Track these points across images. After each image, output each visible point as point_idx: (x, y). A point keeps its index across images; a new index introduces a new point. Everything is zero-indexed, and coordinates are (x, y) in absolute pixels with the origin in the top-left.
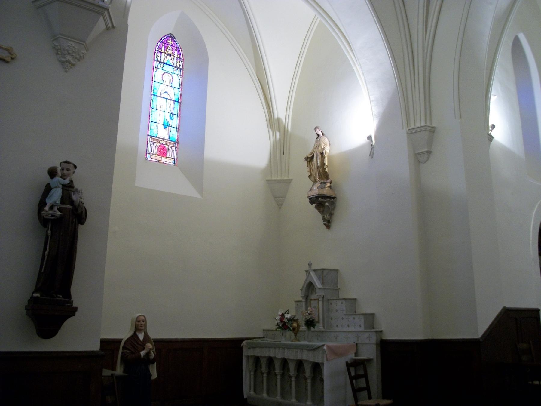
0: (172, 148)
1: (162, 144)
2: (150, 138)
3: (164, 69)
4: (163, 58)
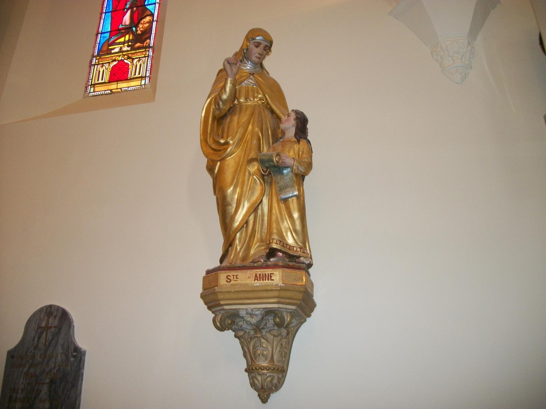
0: (139, 61)
1: (122, 61)
2: (96, 59)
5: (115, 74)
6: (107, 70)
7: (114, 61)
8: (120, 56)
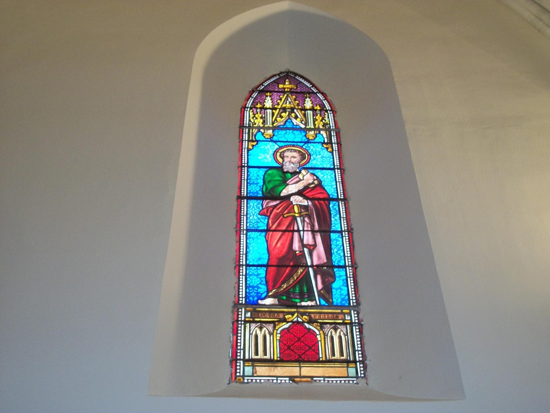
1: (298, 322)
3: (275, 138)
4: (269, 120)
5: (291, 348)
6: (272, 336)
7: (283, 322)
8: (294, 313)
